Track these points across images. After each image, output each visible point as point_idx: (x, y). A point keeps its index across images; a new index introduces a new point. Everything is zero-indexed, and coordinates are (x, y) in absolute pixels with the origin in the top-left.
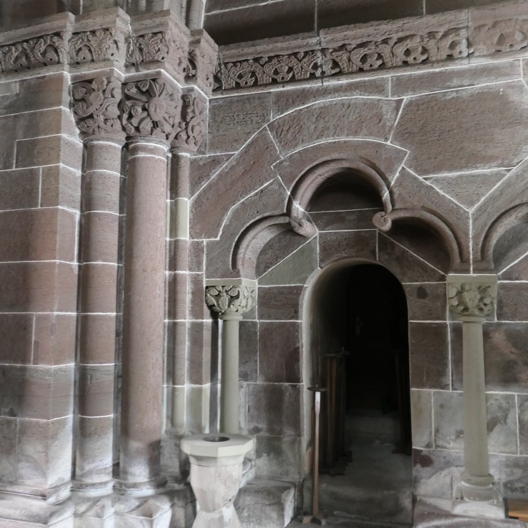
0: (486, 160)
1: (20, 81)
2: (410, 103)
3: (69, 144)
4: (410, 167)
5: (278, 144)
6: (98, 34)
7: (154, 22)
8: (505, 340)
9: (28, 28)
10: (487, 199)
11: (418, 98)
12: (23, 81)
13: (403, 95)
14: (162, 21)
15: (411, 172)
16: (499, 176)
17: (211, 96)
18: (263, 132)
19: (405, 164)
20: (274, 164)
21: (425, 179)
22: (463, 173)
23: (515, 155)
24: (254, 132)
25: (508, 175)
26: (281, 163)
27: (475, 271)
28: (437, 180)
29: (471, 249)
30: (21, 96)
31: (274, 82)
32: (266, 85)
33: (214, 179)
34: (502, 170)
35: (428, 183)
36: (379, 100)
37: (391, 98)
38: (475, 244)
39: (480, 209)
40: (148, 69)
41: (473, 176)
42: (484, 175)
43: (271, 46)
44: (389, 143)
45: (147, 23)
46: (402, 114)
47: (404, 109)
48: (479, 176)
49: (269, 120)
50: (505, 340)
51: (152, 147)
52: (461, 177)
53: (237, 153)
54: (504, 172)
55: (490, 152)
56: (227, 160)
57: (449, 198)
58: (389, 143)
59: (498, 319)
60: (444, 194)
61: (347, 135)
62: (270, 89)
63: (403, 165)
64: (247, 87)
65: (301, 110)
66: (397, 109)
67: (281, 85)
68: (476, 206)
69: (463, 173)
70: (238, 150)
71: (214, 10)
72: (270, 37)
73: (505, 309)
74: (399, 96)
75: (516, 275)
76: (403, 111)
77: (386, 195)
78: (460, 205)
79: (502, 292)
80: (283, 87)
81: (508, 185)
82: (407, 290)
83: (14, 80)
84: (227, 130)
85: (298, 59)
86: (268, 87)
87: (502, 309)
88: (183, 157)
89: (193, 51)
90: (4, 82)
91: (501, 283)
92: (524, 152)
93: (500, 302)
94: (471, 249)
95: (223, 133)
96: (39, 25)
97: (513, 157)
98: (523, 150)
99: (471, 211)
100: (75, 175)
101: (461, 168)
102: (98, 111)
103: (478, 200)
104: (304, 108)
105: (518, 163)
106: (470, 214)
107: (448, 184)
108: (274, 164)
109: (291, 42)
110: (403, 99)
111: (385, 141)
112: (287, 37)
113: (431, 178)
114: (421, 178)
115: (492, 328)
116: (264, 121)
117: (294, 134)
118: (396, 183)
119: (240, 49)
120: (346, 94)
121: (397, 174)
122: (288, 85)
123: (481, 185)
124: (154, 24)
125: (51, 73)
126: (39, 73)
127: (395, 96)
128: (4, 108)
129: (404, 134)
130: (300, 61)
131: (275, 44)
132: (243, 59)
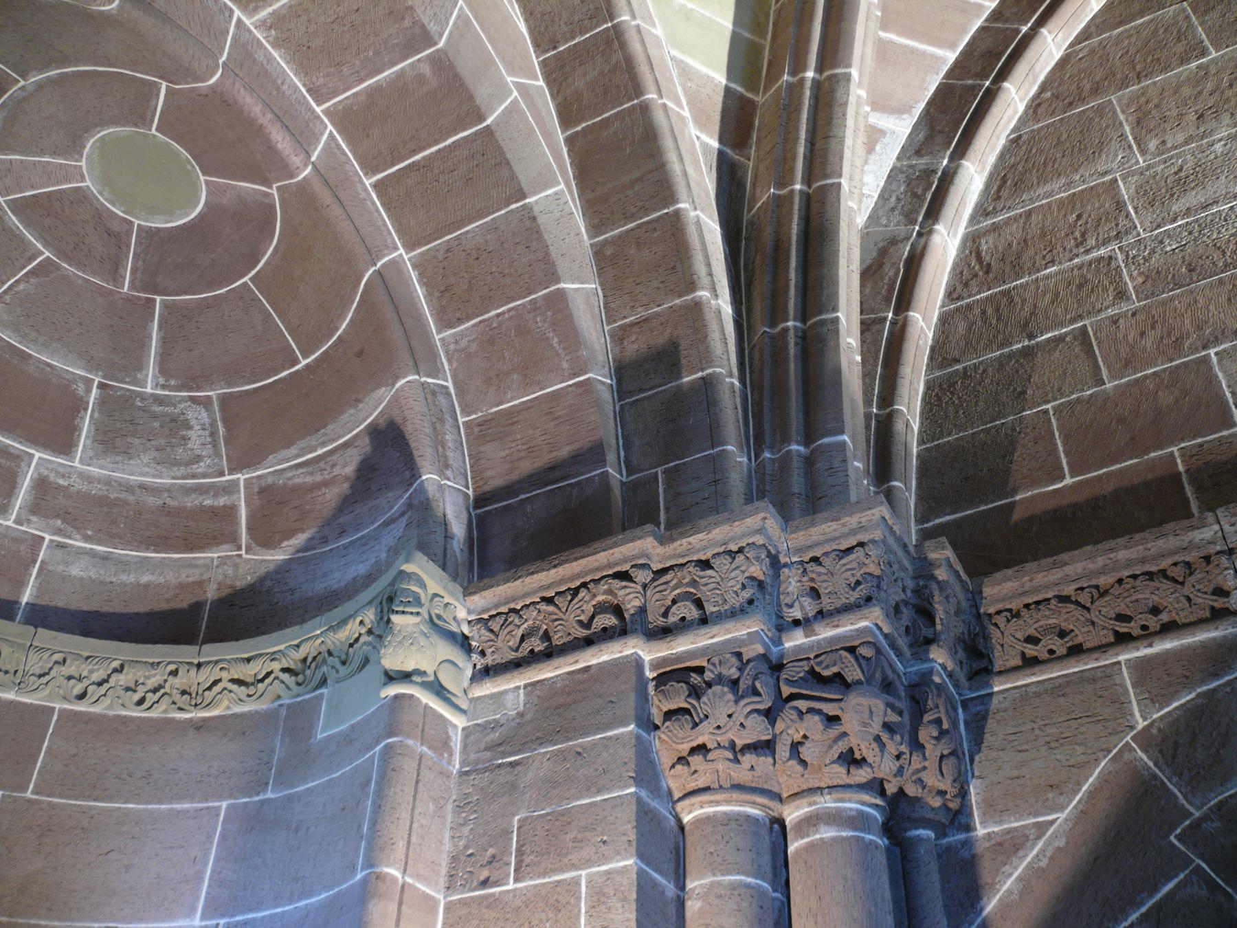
1: (526, 686)
3: (650, 815)
5: (1175, 780)
6: (715, 563)
7: (844, 525)
9: (553, 571)
12: (534, 684)
14: (863, 520)
17: (967, 692)
18: (1127, 756)
20: (1178, 831)
24: (1097, 761)
26: (1197, 824)
30: (528, 717)
31: (1123, 639)
32: (1102, 648)
33: (1009, 891)
40: (837, 626)
43: (1101, 561)
45: (827, 530)
49: (1132, 728)
51: (854, 813)
53: (1062, 816)
56: (1039, 837)
62: (1117, 654)
64: (1053, 658)
65: (1214, 691)
67: (1146, 642)
70: (1062, 808)
71: (937, 517)
72: (1097, 542)
80: (1150, 645)
83: (512, 686)
84: (1022, 765)
85: (1176, 581)
86: (1111, 652)
88: (920, 839)
89: (926, 587)
90: (487, 692)
95: (1015, 773)
96: (581, 561)
100: (663, 892)
102: (723, 730)
104: (1224, 685)
108: (1178, 831)
109: (1149, 546)
112: (1138, 536)
116: (1118, 733)
117: (1213, 751)
119: (1026, 579)
122: (1163, 640)
124: (845, 530)
125: (605, 658)
126: (576, 662)
128: (486, 749)
130: (1182, 584)
131: (1112, 556)
132: (1036, 599)
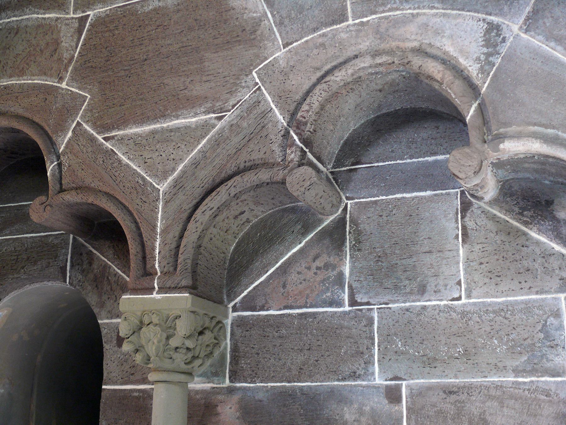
0: (189, 103)
2: (100, 22)
4: (87, 122)
8: (238, 418)
10: (185, 167)
11: (108, 12)
13: (89, 8)
15: (88, 128)
16: (206, 127)
19: (81, 118)
21: (105, 139)
22: (157, 126)
23: (231, 93)
25: (219, 125)
27: (162, 290)
28: (121, 140)
29: (157, 251)
34: (211, 118)
35: (108, 145)
36: (57, 19)
37: (72, 15)
38: (164, 243)
39: (176, 182)
41: (171, 131)
42: (187, 127)
44: (64, 85)
46: (85, 39)
47: (89, 30)
48: (177, 129)
50: (238, 418)
52: (154, 133)
54: (213, 121)
55: (198, 89)
57: (135, 167)
58: (64, 85)
59: (231, 381)
60: (128, 162)
61: (11, 76)
63: (78, 119)
66: (80, 32)
68: (170, 179)
69: (157, 126)
73: (243, 363)
74: (83, 12)
75: (260, 301)
76: (86, 35)
77: (51, 168)
78: (148, 178)
79: (238, 332)
81: (217, 142)
82: (104, 332)
87: (237, 363)
91: (238, 316)
92: (244, 87)
93: (235, 349)
94: (157, 251)
97: (228, 95)
98: (243, 84)
99: (163, 187)
101: (155, 119)
103: (174, 170)
105: (233, 106)
106: (161, 192)
107: (136, 145)
110: (89, 15)
111: (58, 82)
113: (113, 137)
114: (100, 138)
115: (220, 397)
118: (66, 147)
120: (16, 13)
121: (70, 134)
123: (179, 145)
127: (78, 11)
129: (85, 72)
